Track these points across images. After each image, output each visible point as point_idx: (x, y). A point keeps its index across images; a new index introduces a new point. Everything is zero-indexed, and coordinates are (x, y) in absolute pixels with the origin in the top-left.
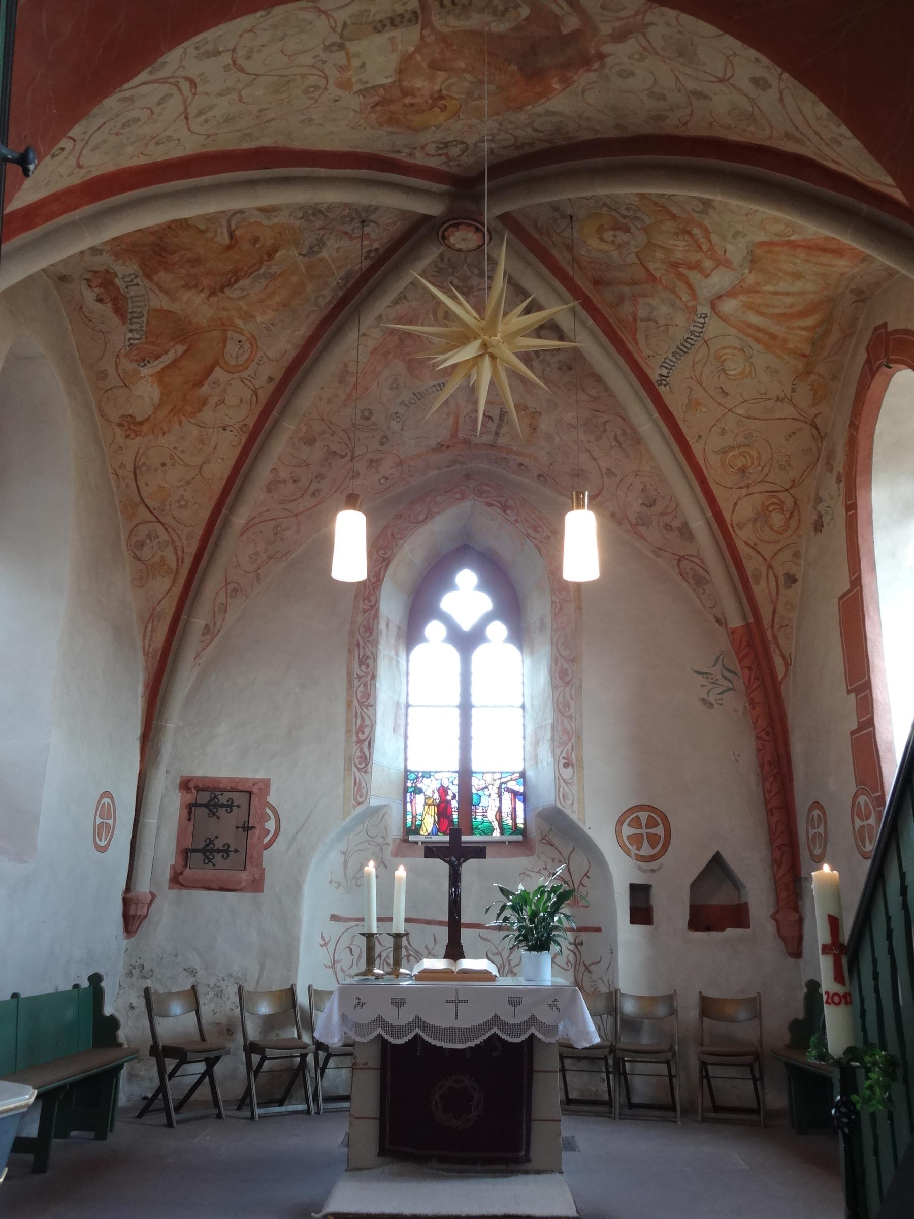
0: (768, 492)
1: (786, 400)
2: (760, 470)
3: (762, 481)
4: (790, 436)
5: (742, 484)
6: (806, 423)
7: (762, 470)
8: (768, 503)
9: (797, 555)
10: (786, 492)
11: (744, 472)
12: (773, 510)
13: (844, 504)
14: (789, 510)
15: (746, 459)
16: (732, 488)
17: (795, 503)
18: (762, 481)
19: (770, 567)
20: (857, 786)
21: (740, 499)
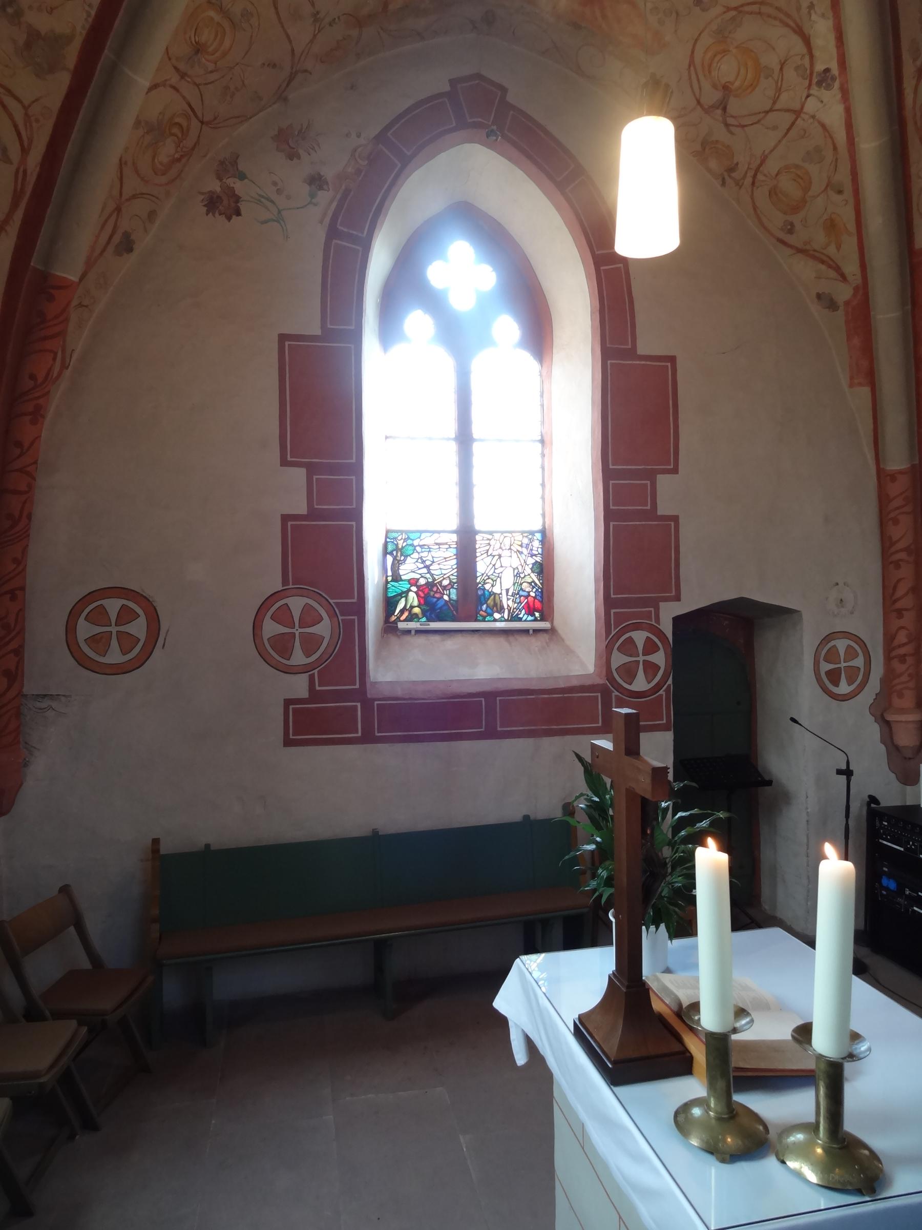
0: (190, 106)
1: (318, 25)
2: (210, 69)
3: (198, 85)
4: (269, 65)
5: (182, 66)
6: (292, 68)
7: (211, 72)
8: (177, 120)
9: (152, 215)
10: (200, 124)
11: (197, 52)
12: (176, 136)
13: (327, 220)
14: (184, 149)
15: (215, 39)
16: (170, 59)
17: (193, 149)
18: (198, 85)
19: (118, 210)
20: (285, 581)
21: (164, 85)
